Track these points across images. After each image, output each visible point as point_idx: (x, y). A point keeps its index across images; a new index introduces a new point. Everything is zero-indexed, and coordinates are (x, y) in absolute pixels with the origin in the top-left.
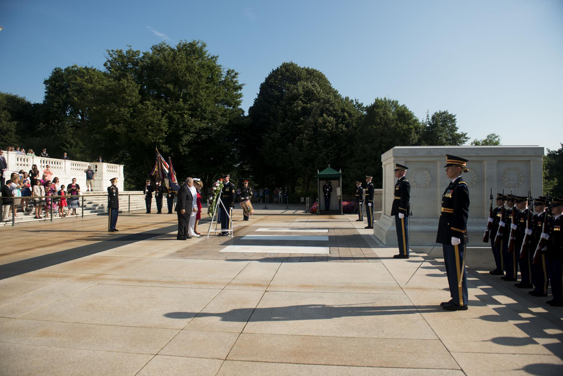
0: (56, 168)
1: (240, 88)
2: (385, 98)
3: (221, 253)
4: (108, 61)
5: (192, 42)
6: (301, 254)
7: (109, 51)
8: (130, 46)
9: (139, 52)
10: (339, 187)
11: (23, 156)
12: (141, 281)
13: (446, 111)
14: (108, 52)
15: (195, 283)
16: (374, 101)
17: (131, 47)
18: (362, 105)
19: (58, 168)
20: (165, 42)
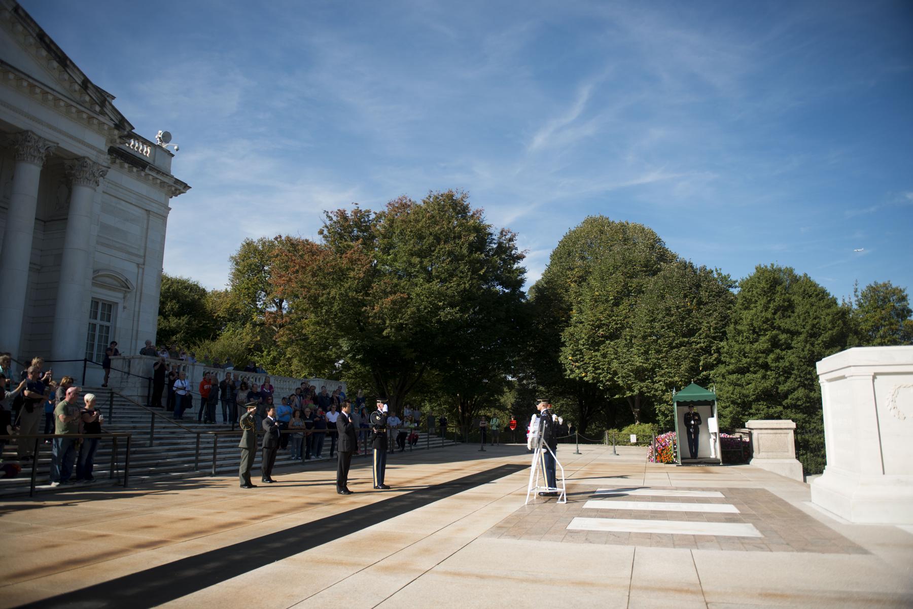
1: (521, 257)
2: (772, 265)
3: (575, 532)
4: (327, 227)
5: (446, 192)
6: (712, 536)
7: (328, 212)
8: (357, 204)
9: (369, 211)
10: (713, 416)
11: (211, 368)
12: (482, 577)
13: (887, 282)
14: (325, 215)
15: (573, 583)
16: (755, 271)
17: (357, 206)
18: (729, 277)
20: (406, 195)
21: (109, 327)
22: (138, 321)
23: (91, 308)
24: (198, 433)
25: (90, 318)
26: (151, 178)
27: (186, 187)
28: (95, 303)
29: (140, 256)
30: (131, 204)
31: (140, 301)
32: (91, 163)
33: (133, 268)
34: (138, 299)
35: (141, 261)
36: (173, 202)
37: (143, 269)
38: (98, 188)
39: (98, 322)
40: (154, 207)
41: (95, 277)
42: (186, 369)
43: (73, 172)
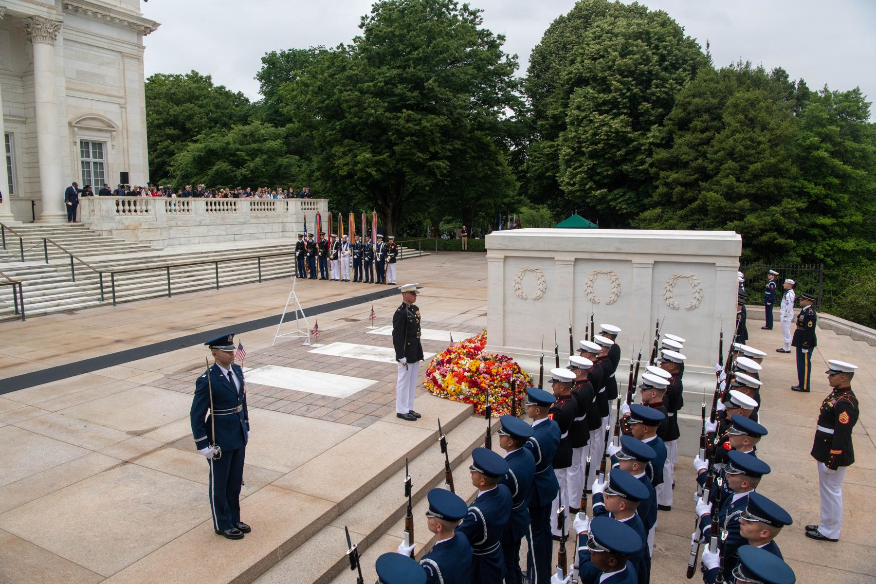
21: (101, 164)
23: (82, 147)
24: (101, 273)
25: (82, 156)
26: (117, 21)
27: (156, 25)
28: (85, 144)
29: (121, 98)
30: (103, 48)
31: (127, 138)
32: (44, 21)
33: (115, 108)
34: (125, 136)
35: (122, 101)
36: (146, 40)
37: (125, 108)
38: (55, 43)
39: (92, 159)
40: (127, 49)
41: (81, 121)
43: (29, 30)
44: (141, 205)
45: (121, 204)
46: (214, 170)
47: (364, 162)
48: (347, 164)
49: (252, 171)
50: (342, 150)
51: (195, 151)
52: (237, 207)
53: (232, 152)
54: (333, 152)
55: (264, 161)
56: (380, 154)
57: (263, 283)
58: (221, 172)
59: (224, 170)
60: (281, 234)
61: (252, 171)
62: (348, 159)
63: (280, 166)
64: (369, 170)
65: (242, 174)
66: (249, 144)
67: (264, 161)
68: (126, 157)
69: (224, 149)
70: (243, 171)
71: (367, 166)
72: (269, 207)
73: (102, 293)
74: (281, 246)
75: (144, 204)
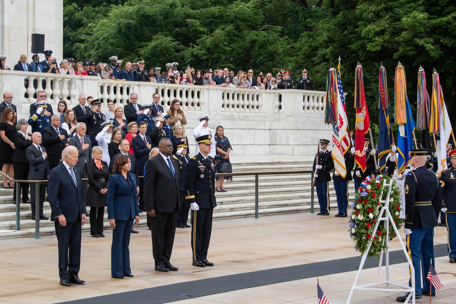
0: (190, 105)
19: (193, 105)
22: (34, 14)
42: (73, 86)
44: (61, 88)
45: (31, 84)
46: (149, 47)
47: (412, 28)
48: (382, 32)
49: (208, 49)
50: (373, 8)
51: (122, 17)
52: (202, 100)
53: (179, 19)
54: (357, 12)
55: (229, 34)
56: (440, 14)
57: (262, 219)
58: (161, 51)
59: (166, 48)
60: (267, 148)
61: (208, 49)
62: (384, 23)
63: (253, 42)
64: (421, 42)
65: (193, 56)
66: (205, 6)
67: (229, 34)
68: (31, 17)
69: (166, 15)
70: (196, 50)
71: (417, 35)
72: (251, 103)
73: (19, 218)
74: (279, 163)
75: (66, 86)
